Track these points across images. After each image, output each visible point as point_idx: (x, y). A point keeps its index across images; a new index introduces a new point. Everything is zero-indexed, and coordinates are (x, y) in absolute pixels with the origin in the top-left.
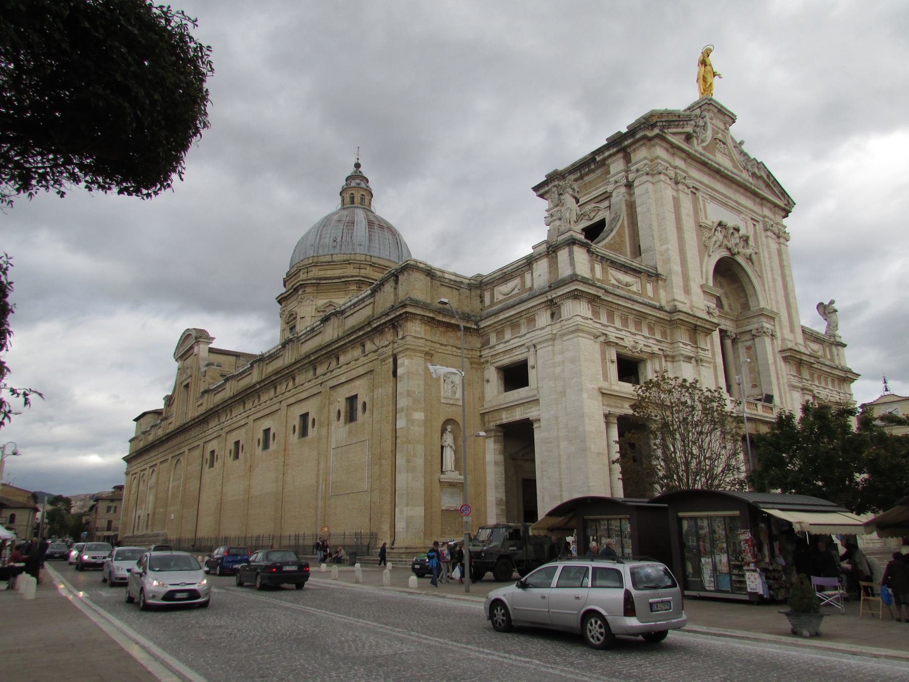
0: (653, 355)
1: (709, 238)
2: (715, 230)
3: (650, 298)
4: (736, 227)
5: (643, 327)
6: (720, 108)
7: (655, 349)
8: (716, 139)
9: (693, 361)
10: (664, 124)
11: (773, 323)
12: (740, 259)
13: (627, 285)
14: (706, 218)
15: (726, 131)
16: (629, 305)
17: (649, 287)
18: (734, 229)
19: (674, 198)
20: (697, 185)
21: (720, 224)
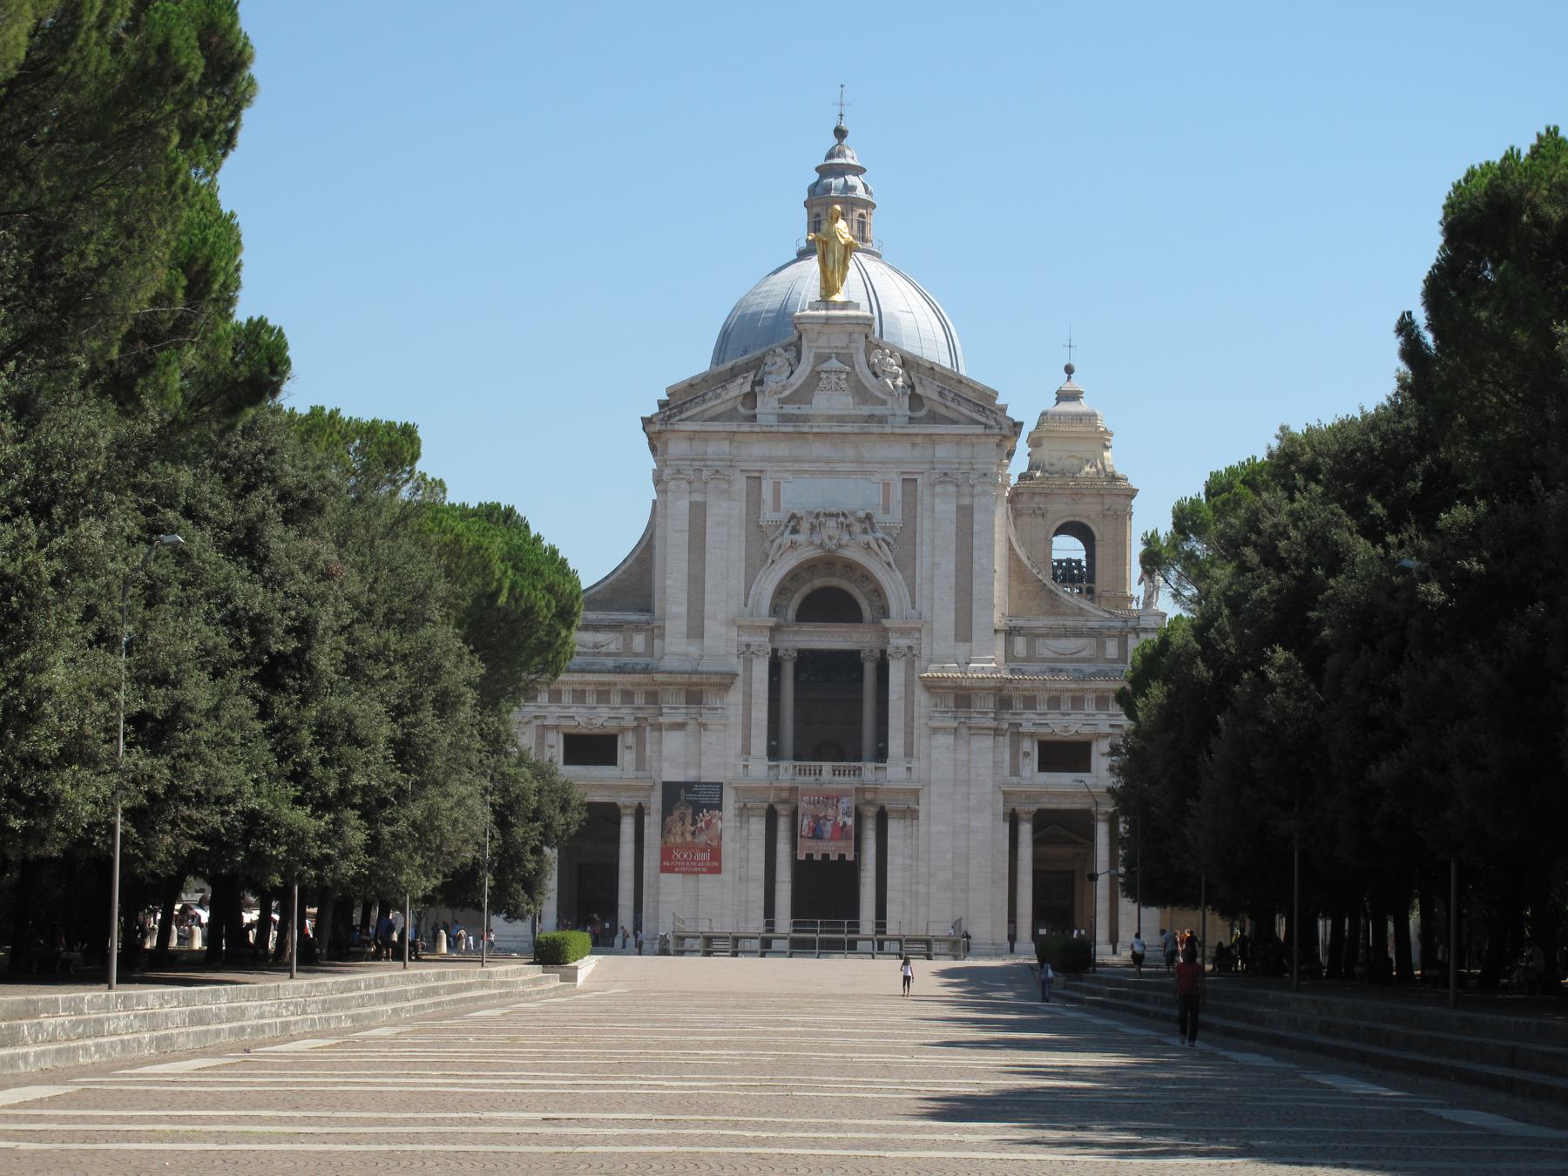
0: (623, 730)
1: (773, 541)
2: (787, 526)
3: (637, 655)
4: (827, 512)
5: (612, 696)
6: (824, 321)
7: (629, 721)
8: (819, 373)
9: (692, 726)
10: (668, 413)
11: (917, 635)
12: (852, 554)
13: (596, 646)
14: (777, 507)
15: (852, 345)
16: (576, 678)
17: (639, 641)
18: (825, 514)
19: (692, 505)
20: (759, 466)
21: (793, 517)
